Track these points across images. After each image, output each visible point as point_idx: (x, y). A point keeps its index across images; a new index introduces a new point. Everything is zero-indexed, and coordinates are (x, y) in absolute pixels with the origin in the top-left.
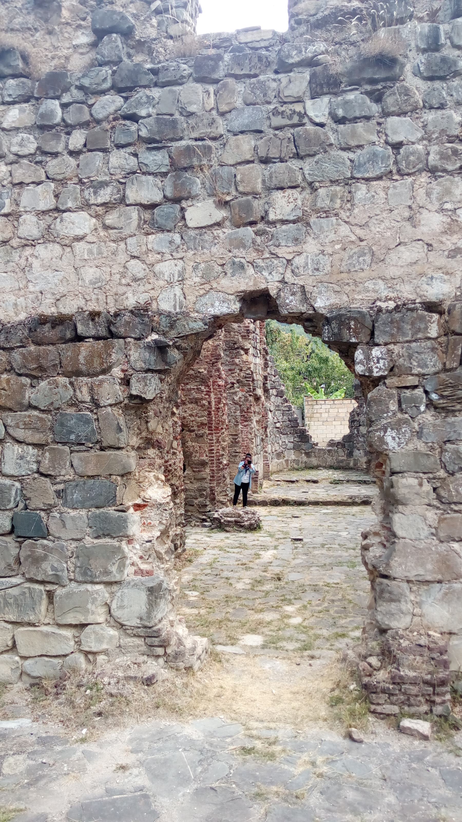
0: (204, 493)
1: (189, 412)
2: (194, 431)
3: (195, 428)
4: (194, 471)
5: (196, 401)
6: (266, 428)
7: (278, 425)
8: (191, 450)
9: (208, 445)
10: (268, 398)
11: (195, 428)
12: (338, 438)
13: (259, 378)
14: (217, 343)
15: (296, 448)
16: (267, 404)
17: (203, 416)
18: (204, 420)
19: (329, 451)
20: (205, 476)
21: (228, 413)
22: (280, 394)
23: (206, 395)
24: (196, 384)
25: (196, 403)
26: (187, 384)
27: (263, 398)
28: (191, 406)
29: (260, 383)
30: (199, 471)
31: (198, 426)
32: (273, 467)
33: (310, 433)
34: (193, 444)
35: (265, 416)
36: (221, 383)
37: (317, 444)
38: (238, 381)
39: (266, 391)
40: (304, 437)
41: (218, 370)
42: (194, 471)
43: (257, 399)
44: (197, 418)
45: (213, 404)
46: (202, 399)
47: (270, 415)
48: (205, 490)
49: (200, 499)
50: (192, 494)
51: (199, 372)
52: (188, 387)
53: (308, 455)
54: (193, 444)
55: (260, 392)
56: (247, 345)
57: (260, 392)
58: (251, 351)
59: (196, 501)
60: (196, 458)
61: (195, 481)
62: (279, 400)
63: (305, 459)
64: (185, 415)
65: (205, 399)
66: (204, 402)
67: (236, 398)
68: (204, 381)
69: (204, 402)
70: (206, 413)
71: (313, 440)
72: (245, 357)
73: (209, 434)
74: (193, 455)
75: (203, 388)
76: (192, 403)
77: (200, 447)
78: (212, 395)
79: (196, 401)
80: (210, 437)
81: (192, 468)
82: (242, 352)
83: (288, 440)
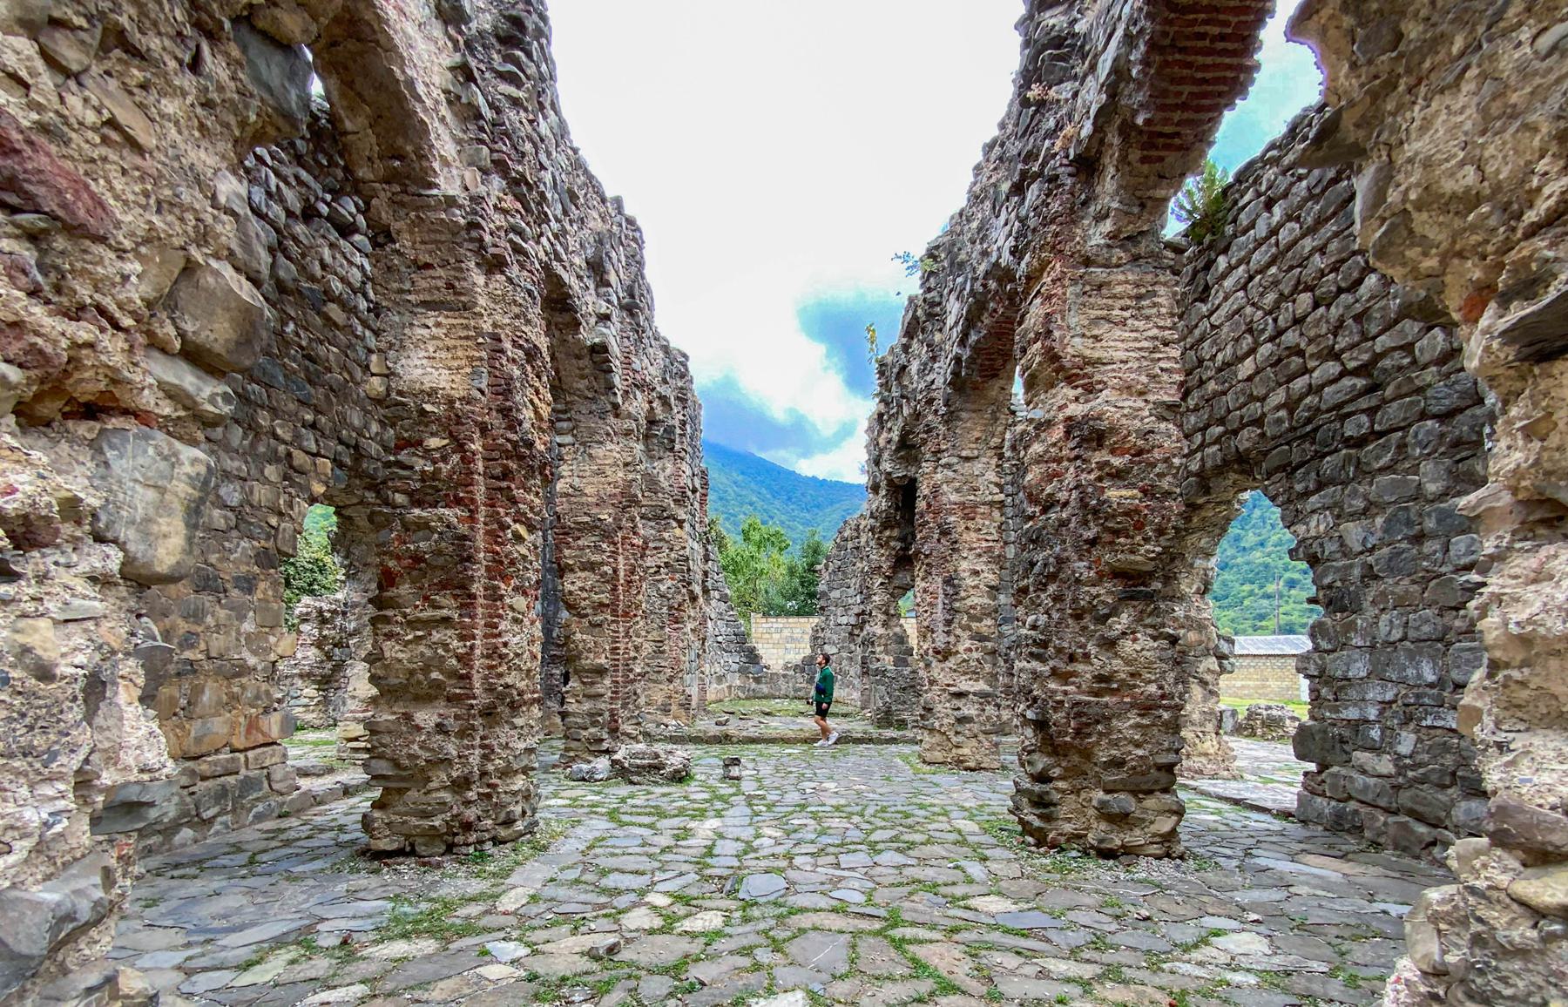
5: (591, 567)
6: (704, 640)
7: (720, 639)
10: (708, 601)
12: (796, 658)
13: (697, 567)
14: (630, 476)
15: (743, 671)
16: (707, 609)
18: (605, 598)
19: (784, 676)
21: (646, 596)
22: (724, 599)
25: (593, 570)
27: (701, 600)
28: (583, 575)
29: (699, 577)
32: (710, 696)
33: (761, 652)
35: (703, 623)
36: (638, 541)
37: (768, 667)
38: (667, 565)
39: (706, 591)
40: (753, 657)
41: (632, 520)
43: (694, 599)
45: (622, 574)
47: (710, 624)
53: (757, 680)
55: (697, 589)
56: (682, 515)
57: (697, 589)
58: (686, 525)
62: (723, 606)
63: (754, 685)
66: (605, 568)
67: (663, 588)
68: (607, 535)
71: (763, 662)
72: (678, 531)
75: (604, 546)
78: (620, 558)
79: (591, 567)
82: (674, 524)
83: (733, 660)
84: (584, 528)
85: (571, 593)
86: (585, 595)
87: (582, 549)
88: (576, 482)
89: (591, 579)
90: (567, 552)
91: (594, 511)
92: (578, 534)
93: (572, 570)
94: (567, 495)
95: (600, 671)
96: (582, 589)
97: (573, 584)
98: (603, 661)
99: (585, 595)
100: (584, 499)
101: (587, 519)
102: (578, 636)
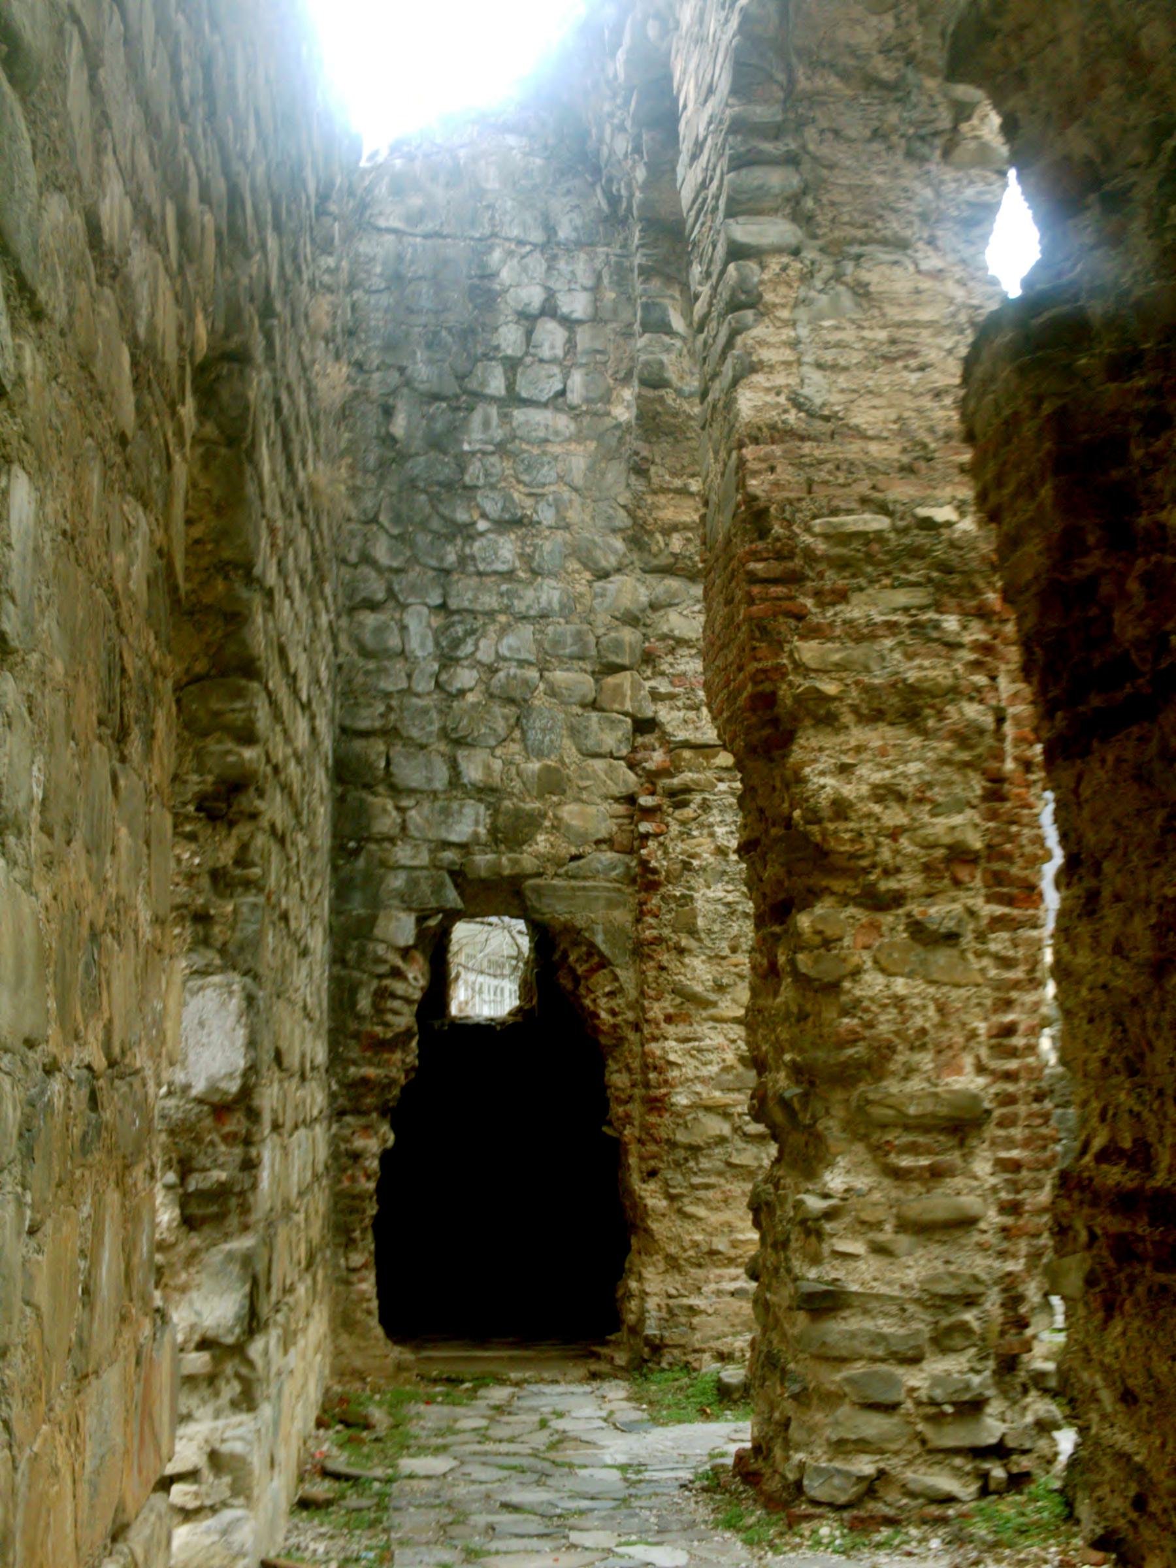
0: (969, 1316)
1: (871, 774)
2: (898, 899)
3: (911, 881)
4: (898, 1174)
8: (885, 1026)
9: (988, 996)
11: (911, 881)
17: (960, 805)
18: (965, 826)
20: (971, 1202)
23: (976, 665)
24: (902, 597)
26: (842, 596)
28: (874, 736)
30: (936, 1174)
31: (927, 868)
34: (900, 985)
42: (898, 1174)
44: (923, 814)
46: (954, 692)
48: (970, 1301)
49: (938, 1366)
50: (887, 1326)
51: (928, 524)
52: (855, 611)
54: (900, 985)
59: (916, 1379)
60: (916, 1084)
61: (904, 1241)
64: (848, 791)
65: (976, 694)
69: (972, 710)
70: (977, 785)
73: (997, 923)
74: (902, 1057)
75: (951, 623)
76: (875, 716)
77: (941, 1010)
79: (910, 707)
80: (999, 942)
81: (879, 1151)
84: (863, 559)
85: (841, 808)
86: (894, 816)
87: (863, 634)
88: (818, 388)
89: (914, 760)
90: (809, 651)
91: (899, 491)
92: (832, 579)
93: (829, 721)
94: (779, 433)
95: (961, 1125)
96: (886, 793)
97: (838, 770)
98: (967, 1081)
99: (894, 816)
100: (853, 450)
101: (880, 523)
102: (873, 984)
